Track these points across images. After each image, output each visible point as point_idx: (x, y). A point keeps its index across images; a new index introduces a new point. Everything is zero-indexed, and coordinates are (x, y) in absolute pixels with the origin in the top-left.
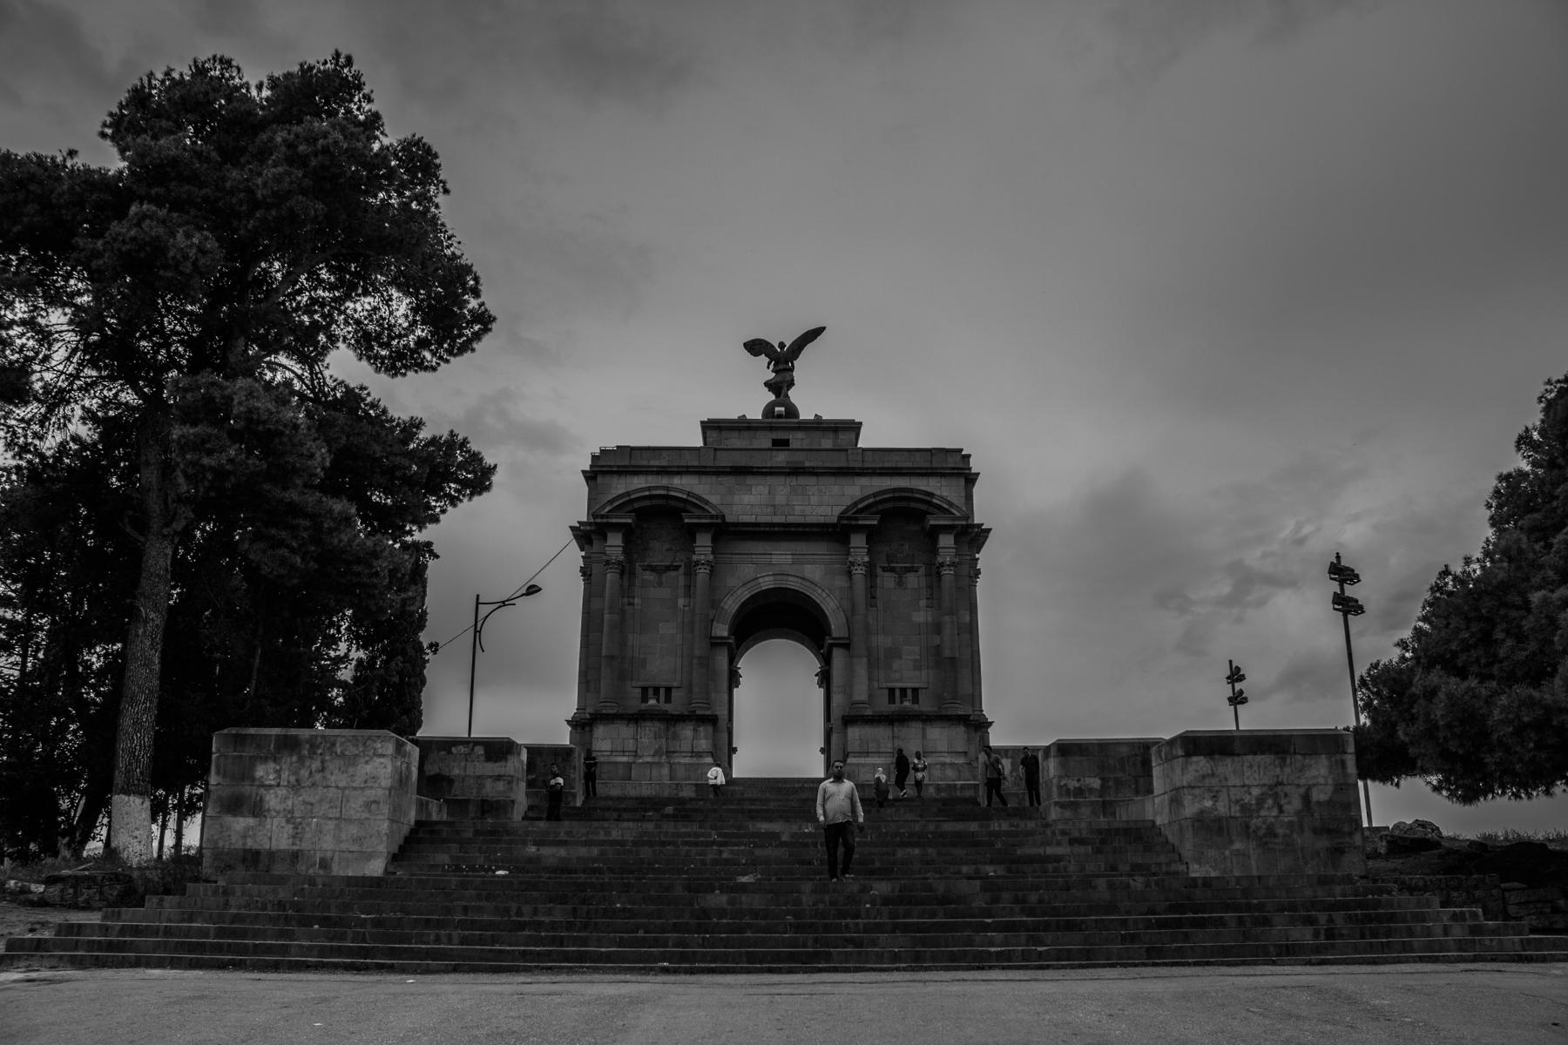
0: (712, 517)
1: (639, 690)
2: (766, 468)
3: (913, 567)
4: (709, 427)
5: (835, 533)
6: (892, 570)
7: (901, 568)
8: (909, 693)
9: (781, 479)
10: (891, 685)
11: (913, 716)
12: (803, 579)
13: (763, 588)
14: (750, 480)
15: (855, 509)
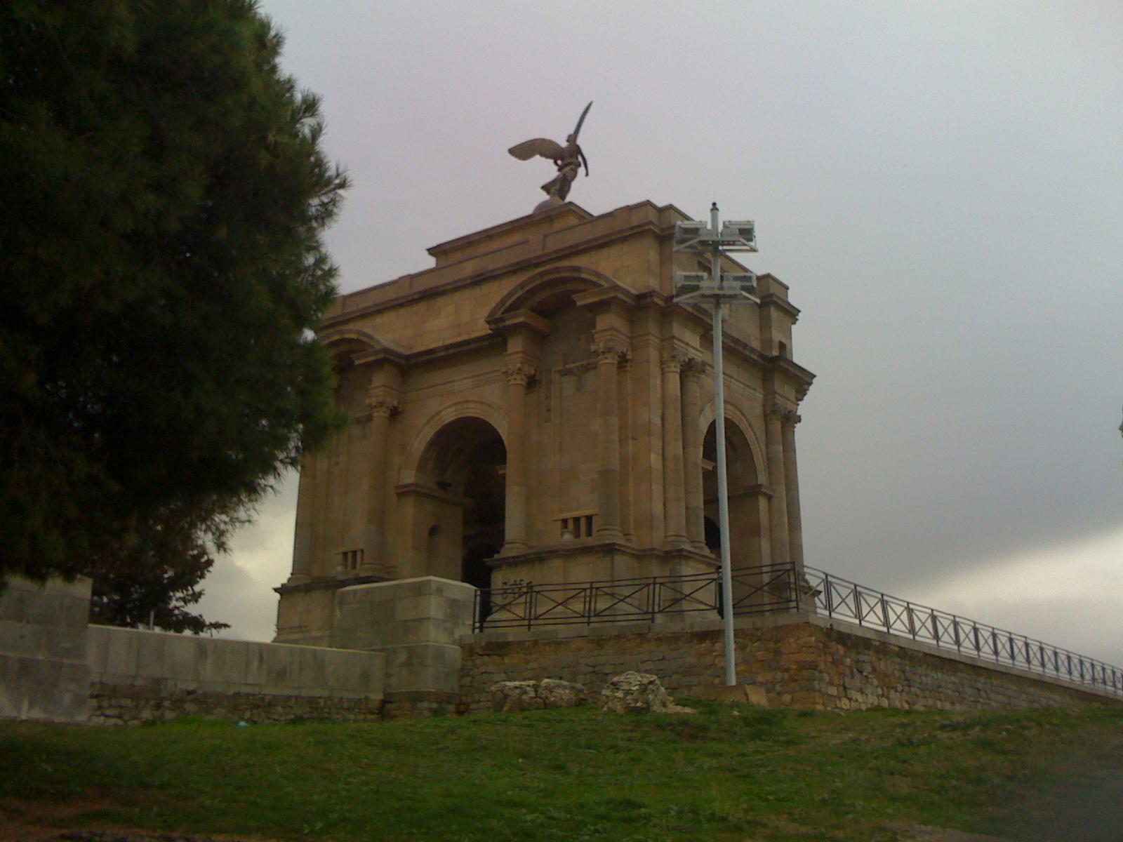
0: (377, 352)
1: (341, 556)
2: (448, 284)
3: (589, 364)
4: (432, 251)
5: (494, 342)
6: (569, 372)
7: (578, 367)
8: (571, 524)
9: (466, 294)
10: (564, 516)
11: (552, 552)
12: (483, 403)
13: (447, 422)
14: (440, 302)
15: (502, 310)
